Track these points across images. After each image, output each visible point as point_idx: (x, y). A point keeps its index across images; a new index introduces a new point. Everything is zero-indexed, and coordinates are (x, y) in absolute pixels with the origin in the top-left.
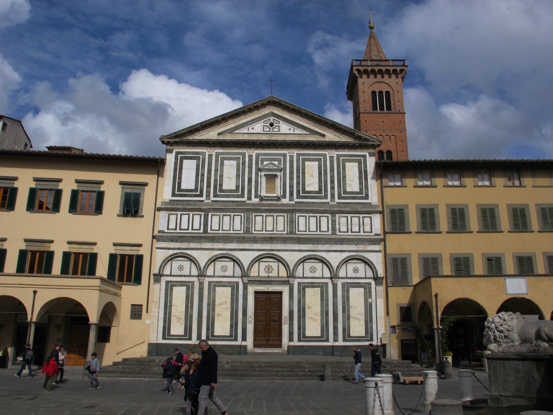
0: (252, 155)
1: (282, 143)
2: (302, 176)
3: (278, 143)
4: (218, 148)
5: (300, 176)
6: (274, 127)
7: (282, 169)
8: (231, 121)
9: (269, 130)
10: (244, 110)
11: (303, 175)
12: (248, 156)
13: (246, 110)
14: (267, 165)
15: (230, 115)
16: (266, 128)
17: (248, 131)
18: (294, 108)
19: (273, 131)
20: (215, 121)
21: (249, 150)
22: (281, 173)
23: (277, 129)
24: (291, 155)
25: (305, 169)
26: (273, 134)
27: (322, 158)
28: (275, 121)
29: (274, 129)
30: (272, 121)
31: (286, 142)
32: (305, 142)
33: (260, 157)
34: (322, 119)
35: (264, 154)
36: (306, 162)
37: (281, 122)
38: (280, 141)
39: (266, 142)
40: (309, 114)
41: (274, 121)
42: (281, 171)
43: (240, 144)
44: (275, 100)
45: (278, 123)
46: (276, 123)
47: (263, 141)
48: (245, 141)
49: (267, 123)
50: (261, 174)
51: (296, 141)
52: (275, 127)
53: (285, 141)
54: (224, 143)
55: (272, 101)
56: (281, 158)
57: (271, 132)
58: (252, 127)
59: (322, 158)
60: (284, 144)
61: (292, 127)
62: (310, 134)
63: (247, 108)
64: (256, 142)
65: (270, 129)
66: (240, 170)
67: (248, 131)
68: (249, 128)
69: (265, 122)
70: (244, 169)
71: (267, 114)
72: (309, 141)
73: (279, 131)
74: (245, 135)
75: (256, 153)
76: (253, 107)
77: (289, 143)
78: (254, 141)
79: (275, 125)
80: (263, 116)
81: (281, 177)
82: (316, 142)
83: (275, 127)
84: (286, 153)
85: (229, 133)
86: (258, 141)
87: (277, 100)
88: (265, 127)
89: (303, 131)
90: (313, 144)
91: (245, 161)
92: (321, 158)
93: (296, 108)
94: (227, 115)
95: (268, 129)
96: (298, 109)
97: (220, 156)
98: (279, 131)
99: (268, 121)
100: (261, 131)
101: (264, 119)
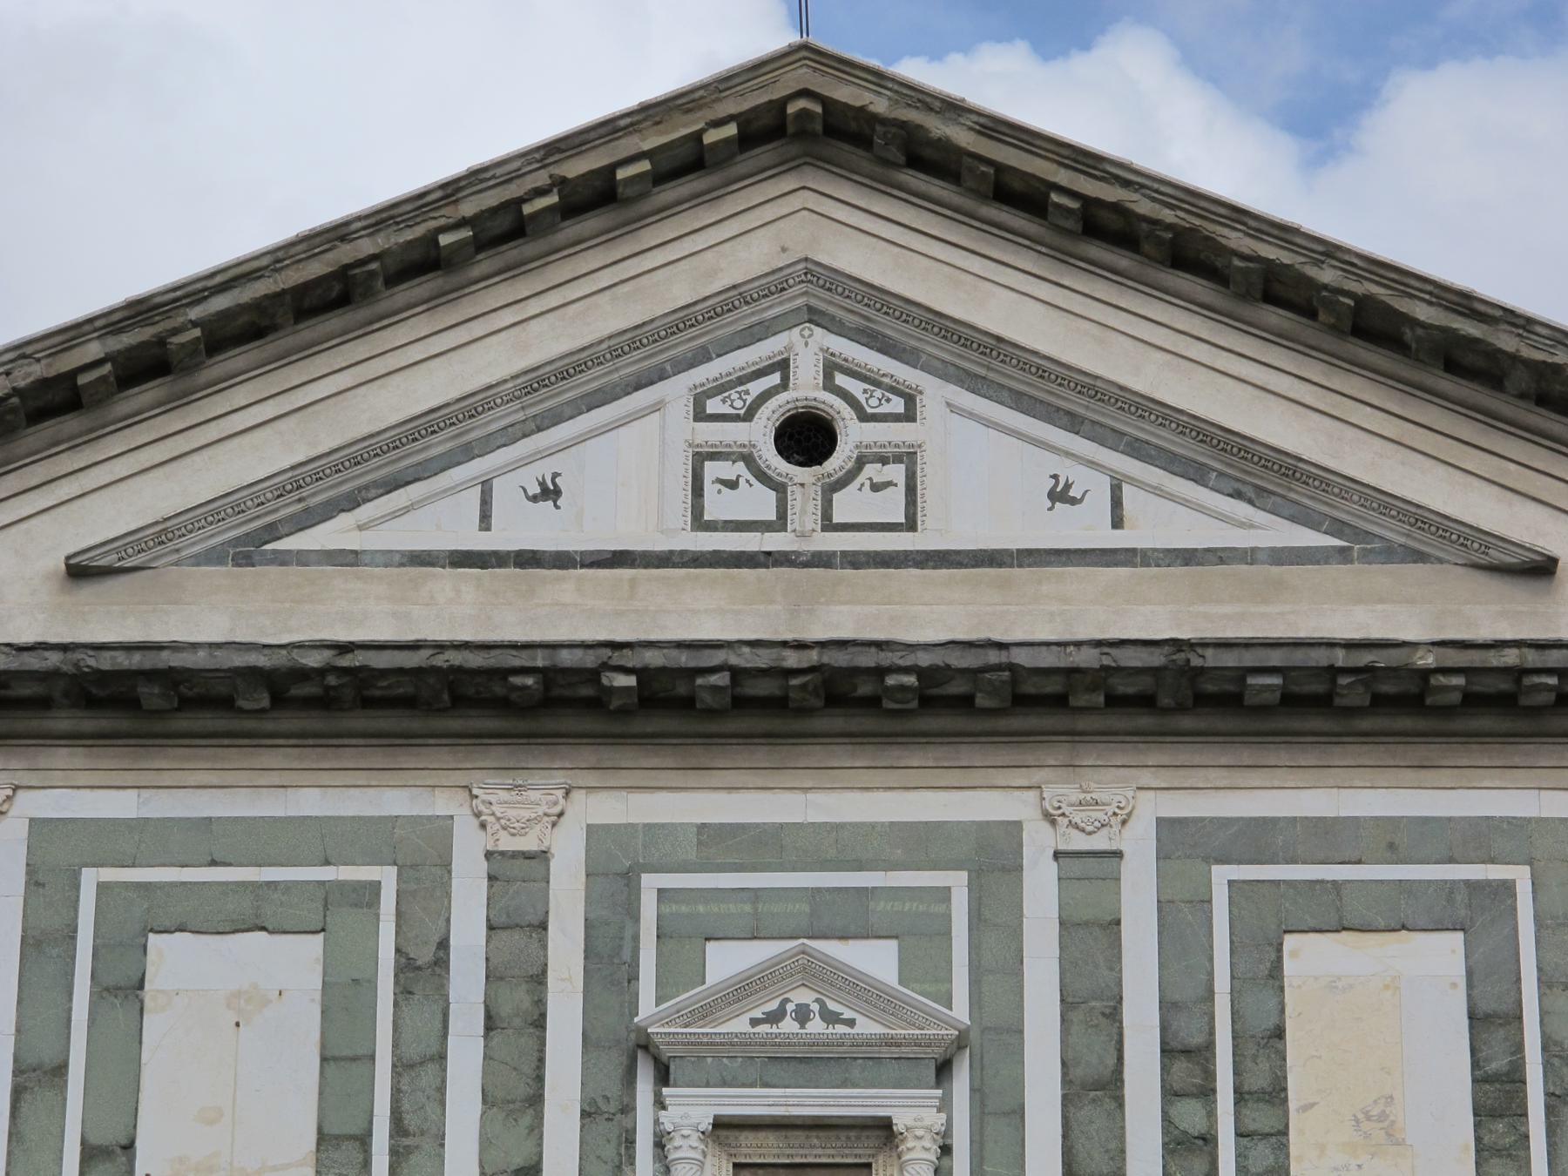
0: (543, 856)
1: (957, 688)
2: (1239, 1134)
3: (891, 680)
4: (62, 757)
5: (1208, 1140)
6: (837, 462)
7: (961, 1042)
8: (240, 396)
10: (431, 239)
11: (1261, 1118)
12: (483, 866)
13: (445, 240)
14: (743, 989)
15: (242, 309)
16: (732, 485)
17: (485, 521)
18: (1117, 208)
19: (829, 525)
20: (16, 391)
21: (496, 795)
22: (945, 1105)
23: (876, 487)
24: (1079, 843)
25: (1279, 1033)
26: (821, 560)
27: (1521, 876)
28: (855, 387)
29: (836, 496)
30: (806, 389)
31: (1012, 668)
32: (1275, 658)
33: (650, 883)
34: (1506, 341)
35: (709, 835)
36: (1290, 942)
37: (935, 392)
38: (924, 660)
39: (737, 673)
40: (1327, 275)
41: (841, 380)
42: (943, 1069)
43: (368, 703)
44: (846, 93)
45: (897, 405)
46: (864, 417)
47: (684, 659)
48: (440, 661)
49: (748, 416)
50: (668, 1119)
51: (1156, 659)
52: (861, 462)
53: (994, 657)
54: (150, 694)
55: (804, 114)
56: (944, 894)
57: (802, 535)
58: (544, 469)
59: (1521, 876)
60: (981, 701)
61: (1092, 464)
62: (1343, 555)
63: (468, 209)
64: (593, 675)
65: (780, 488)
66: (372, 1058)
67: (485, 521)
69: (714, 406)
70: (434, 1050)
71: (737, 297)
72: (1331, 644)
73: (911, 525)
74: (445, 580)
75: (591, 830)
76: (553, 199)
77: (1053, 686)
78: (567, 658)
79: (852, 435)
80: (683, 320)
81: (946, 1150)
82: (1428, 660)
83: (861, 462)
84: (1018, 825)
85: (213, 557)
86: (618, 658)
87: (880, 105)
88: (712, 470)
89: (1241, 509)
90: (1387, 688)
91: (444, 944)
92: (1508, 888)
93: (1144, 207)
94: (194, 313)
95: (757, 502)
96: (1168, 216)
97: (90, 879)
98: (911, 525)
99: (756, 387)
101: (703, 356)
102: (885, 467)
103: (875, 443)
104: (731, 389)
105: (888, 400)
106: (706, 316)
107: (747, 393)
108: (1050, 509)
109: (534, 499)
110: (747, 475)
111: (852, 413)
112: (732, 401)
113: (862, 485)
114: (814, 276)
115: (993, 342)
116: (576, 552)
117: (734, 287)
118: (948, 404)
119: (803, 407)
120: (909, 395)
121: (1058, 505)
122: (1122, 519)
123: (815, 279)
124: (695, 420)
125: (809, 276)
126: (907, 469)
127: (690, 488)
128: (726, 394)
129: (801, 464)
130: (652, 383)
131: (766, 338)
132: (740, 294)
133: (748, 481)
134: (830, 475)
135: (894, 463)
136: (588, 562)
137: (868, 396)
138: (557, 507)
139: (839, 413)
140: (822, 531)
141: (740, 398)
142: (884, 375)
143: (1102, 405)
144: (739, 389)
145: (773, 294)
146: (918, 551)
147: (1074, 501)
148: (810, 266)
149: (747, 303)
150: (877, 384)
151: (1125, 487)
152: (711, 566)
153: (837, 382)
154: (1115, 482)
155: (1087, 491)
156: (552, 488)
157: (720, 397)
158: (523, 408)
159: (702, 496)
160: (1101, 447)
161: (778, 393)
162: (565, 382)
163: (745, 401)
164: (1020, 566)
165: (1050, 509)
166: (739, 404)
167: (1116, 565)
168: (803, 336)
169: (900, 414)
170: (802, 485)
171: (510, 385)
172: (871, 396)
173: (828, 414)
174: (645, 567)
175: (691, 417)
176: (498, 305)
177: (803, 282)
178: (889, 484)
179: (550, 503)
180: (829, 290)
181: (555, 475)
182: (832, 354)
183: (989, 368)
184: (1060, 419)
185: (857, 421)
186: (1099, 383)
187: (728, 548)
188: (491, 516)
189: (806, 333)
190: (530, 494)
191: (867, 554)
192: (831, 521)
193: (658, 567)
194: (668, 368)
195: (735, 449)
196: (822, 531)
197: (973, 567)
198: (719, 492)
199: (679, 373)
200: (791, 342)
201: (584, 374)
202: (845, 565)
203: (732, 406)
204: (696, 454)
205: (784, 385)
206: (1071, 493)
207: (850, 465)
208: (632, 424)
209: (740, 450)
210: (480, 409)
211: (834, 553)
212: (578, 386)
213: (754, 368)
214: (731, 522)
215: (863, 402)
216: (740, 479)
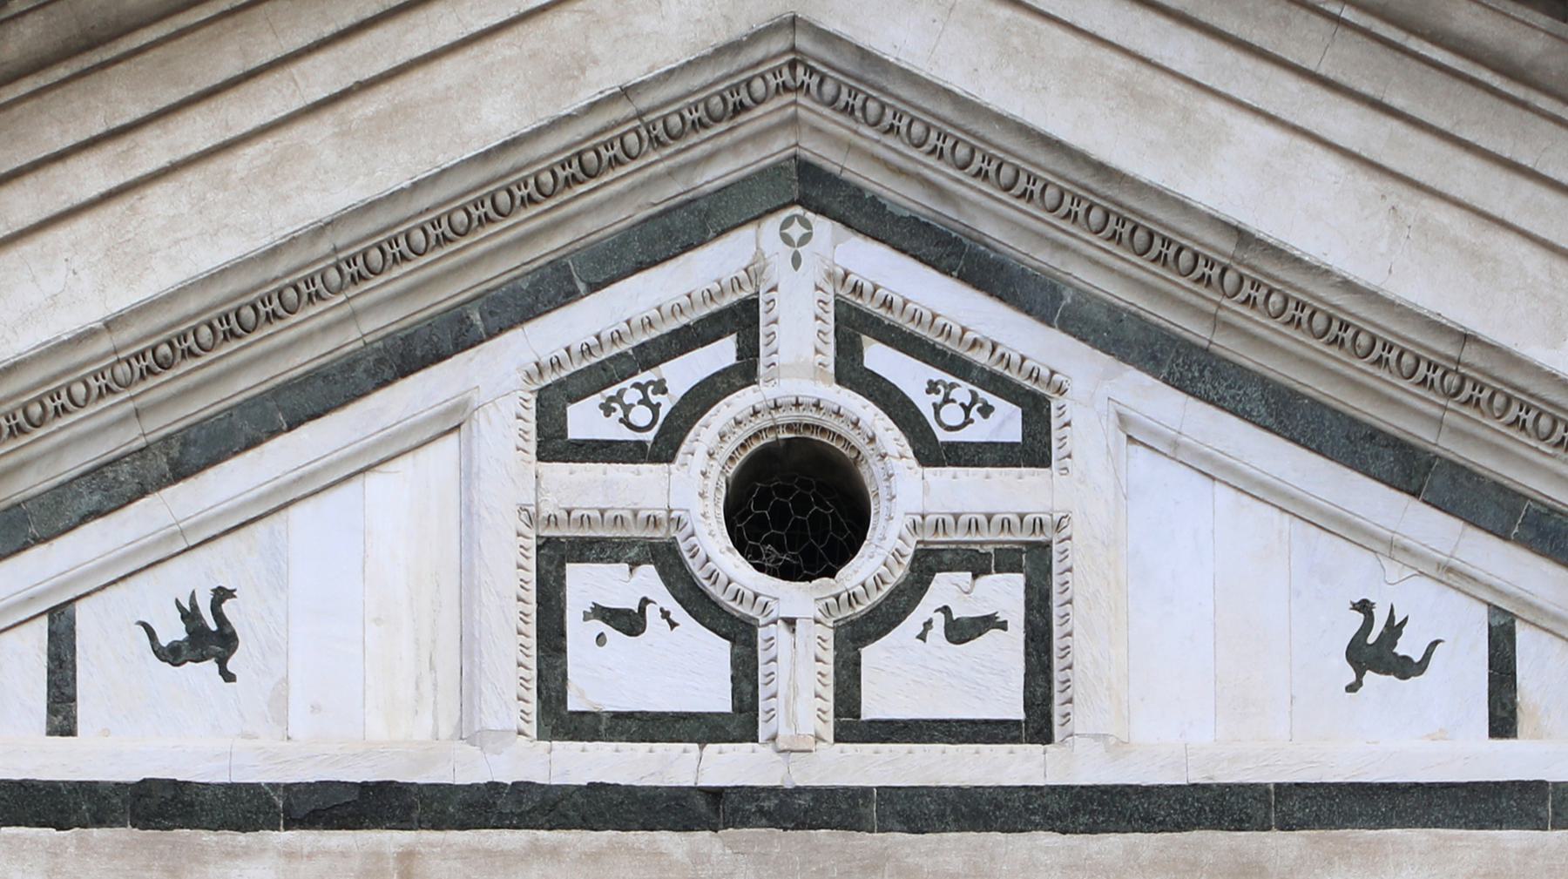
9: (720, 700)
16: (630, 622)
23: (961, 631)
29: (872, 655)
41: (879, 358)
46: (931, 452)
49: (664, 448)
61: (1450, 574)
68: (84, 615)
99: (683, 373)
100: (469, 734)
102: (984, 580)
103: (956, 517)
104: (623, 379)
105: (986, 410)
106: (561, 174)
107: (661, 388)
108: (1351, 688)
109: (172, 655)
110: (663, 598)
111: (904, 441)
112: (627, 408)
113: (928, 625)
114: (811, 71)
115: (1228, 246)
116: (274, 786)
117: (626, 93)
118: (1123, 420)
119: (789, 427)
120: (1033, 395)
121: (1370, 677)
122: (1513, 714)
123: (815, 79)
124: (540, 458)
125: (800, 70)
126: (1028, 587)
127: (532, 630)
128: (612, 391)
129: (787, 573)
130: (440, 358)
131: (702, 242)
132: (640, 115)
133: (665, 615)
134: (853, 599)
135: (998, 571)
136: (300, 812)
137: (939, 398)
138: (228, 677)
139: (872, 440)
140: (837, 740)
141: (645, 401)
142: (975, 343)
143: (1475, 415)
144: (643, 377)
145: (718, 120)
146: (1053, 789)
147: (1406, 669)
148: (804, 42)
149: (657, 142)
150: (959, 367)
151: (1522, 634)
152: (587, 824)
153: (868, 364)
154: (1499, 620)
155: (1436, 643)
156: (213, 626)
157: (597, 399)
158: (138, 413)
159: (561, 650)
160: (1470, 531)
161: (733, 389)
162: (234, 345)
163: (655, 409)
164: (1285, 826)
165: (1351, 688)
166: (641, 416)
167: (1499, 824)
168: (787, 240)
169: (1013, 445)
170: (791, 623)
171: (104, 344)
172: (947, 400)
173: (847, 443)
174: (436, 826)
175: (532, 447)
176: (69, 141)
177: (785, 88)
178: (989, 622)
179: (211, 666)
180: (848, 110)
181: (221, 595)
182: (857, 290)
183: (1217, 323)
184: (1377, 456)
185: (913, 462)
186: (1470, 355)
187: (623, 781)
188: (74, 700)
189: (796, 231)
190: (164, 641)
191: (939, 792)
192: (859, 716)
193: (463, 826)
194: (476, 317)
195: (636, 532)
196: (837, 740)
197: (1179, 828)
198: (601, 640)
199: (501, 331)
200: (759, 254)
201: (278, 325)
202: (890, 822)
203: (625, 421)
204: (545, 544)
205: (745, 372)
206: (1400, 650)
207: (899, 573)
208: (391, 466)
209: (649, 533)
210: (36, 410)
211: (865, 792)
212: (266, 356)
213: (674, 324)
214: (630, 715)
215: (929, 415)
216: (649, 607)
